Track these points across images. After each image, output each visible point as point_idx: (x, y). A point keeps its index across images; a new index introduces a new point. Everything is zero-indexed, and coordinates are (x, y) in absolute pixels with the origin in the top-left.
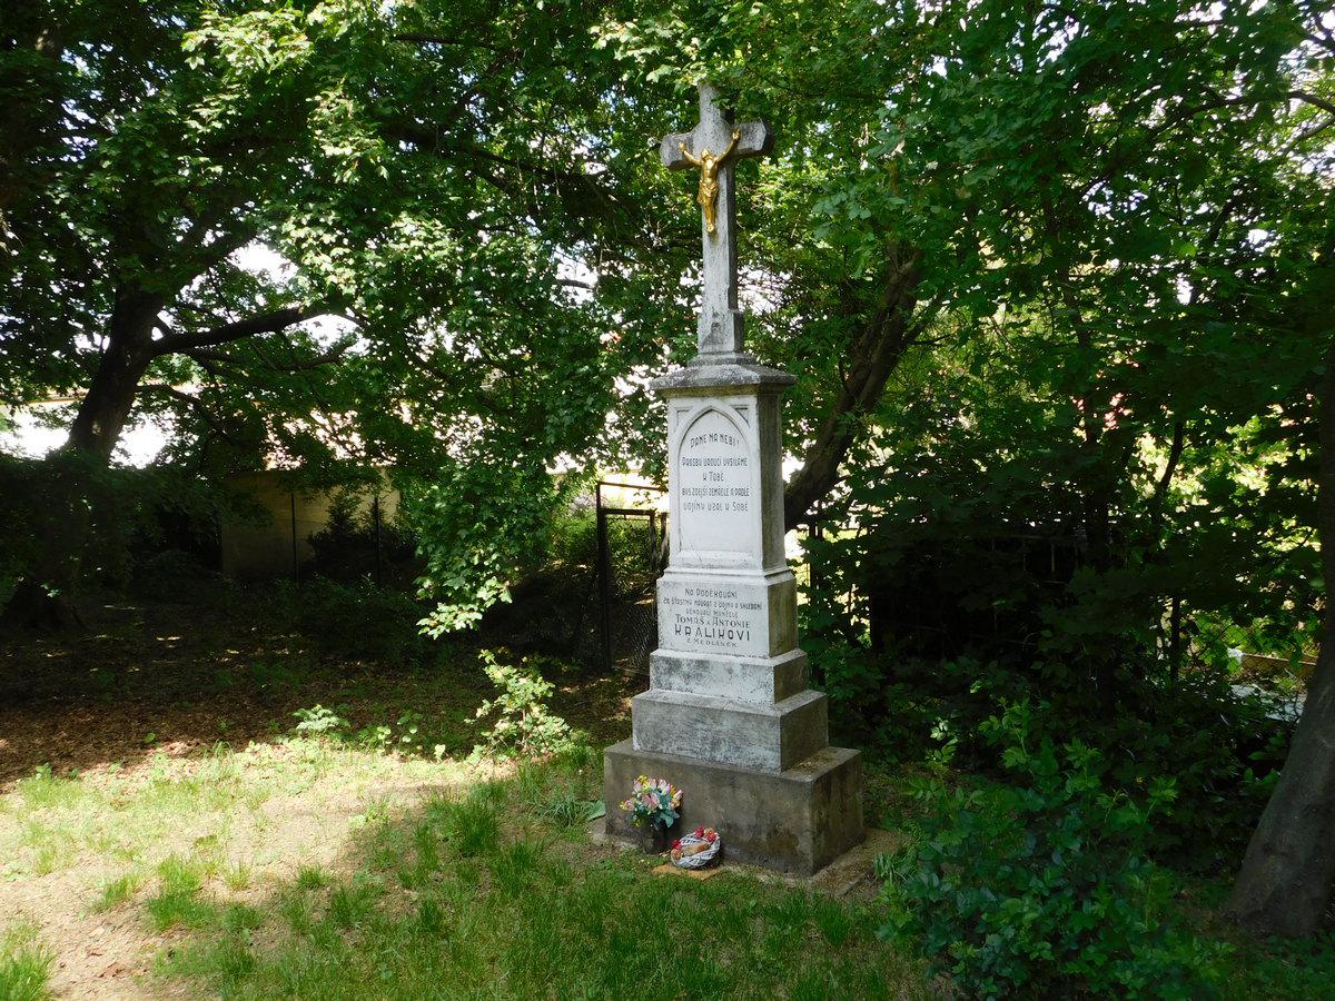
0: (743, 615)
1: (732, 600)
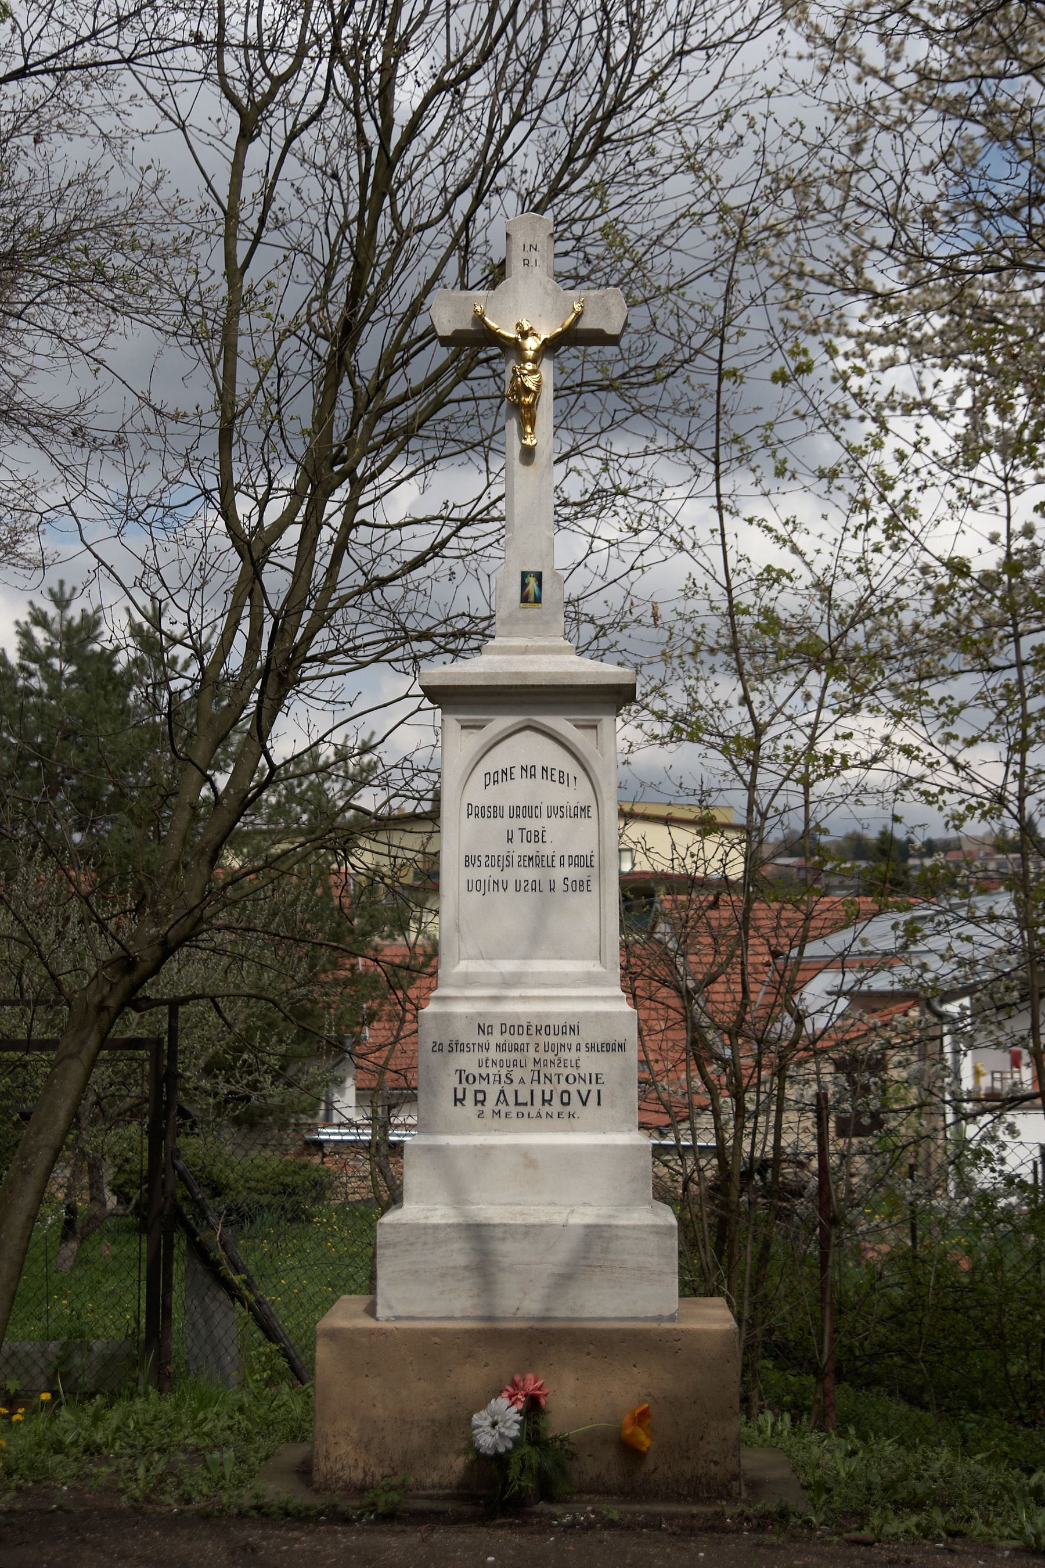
0: (590, 1063)
1: (570, 1039)
